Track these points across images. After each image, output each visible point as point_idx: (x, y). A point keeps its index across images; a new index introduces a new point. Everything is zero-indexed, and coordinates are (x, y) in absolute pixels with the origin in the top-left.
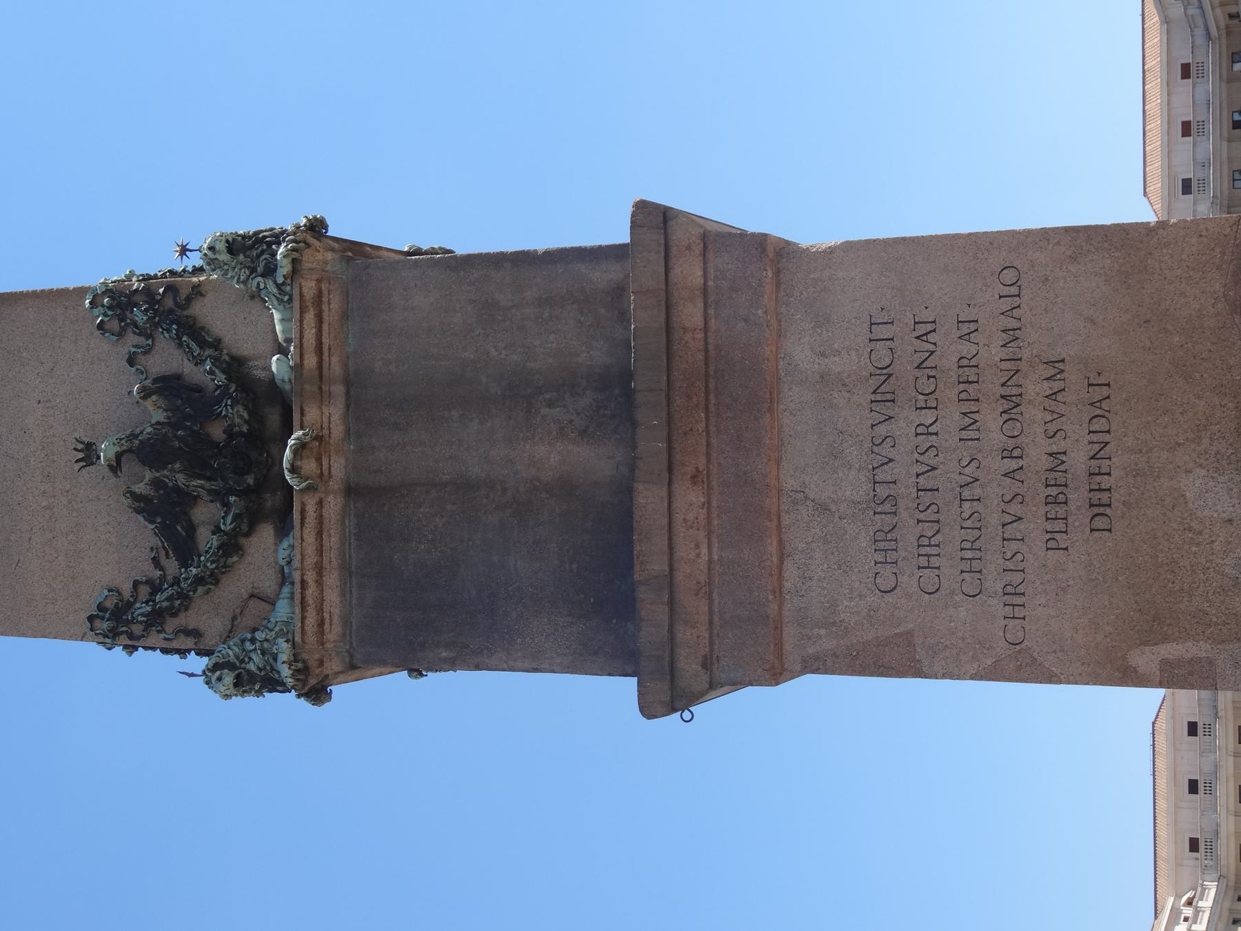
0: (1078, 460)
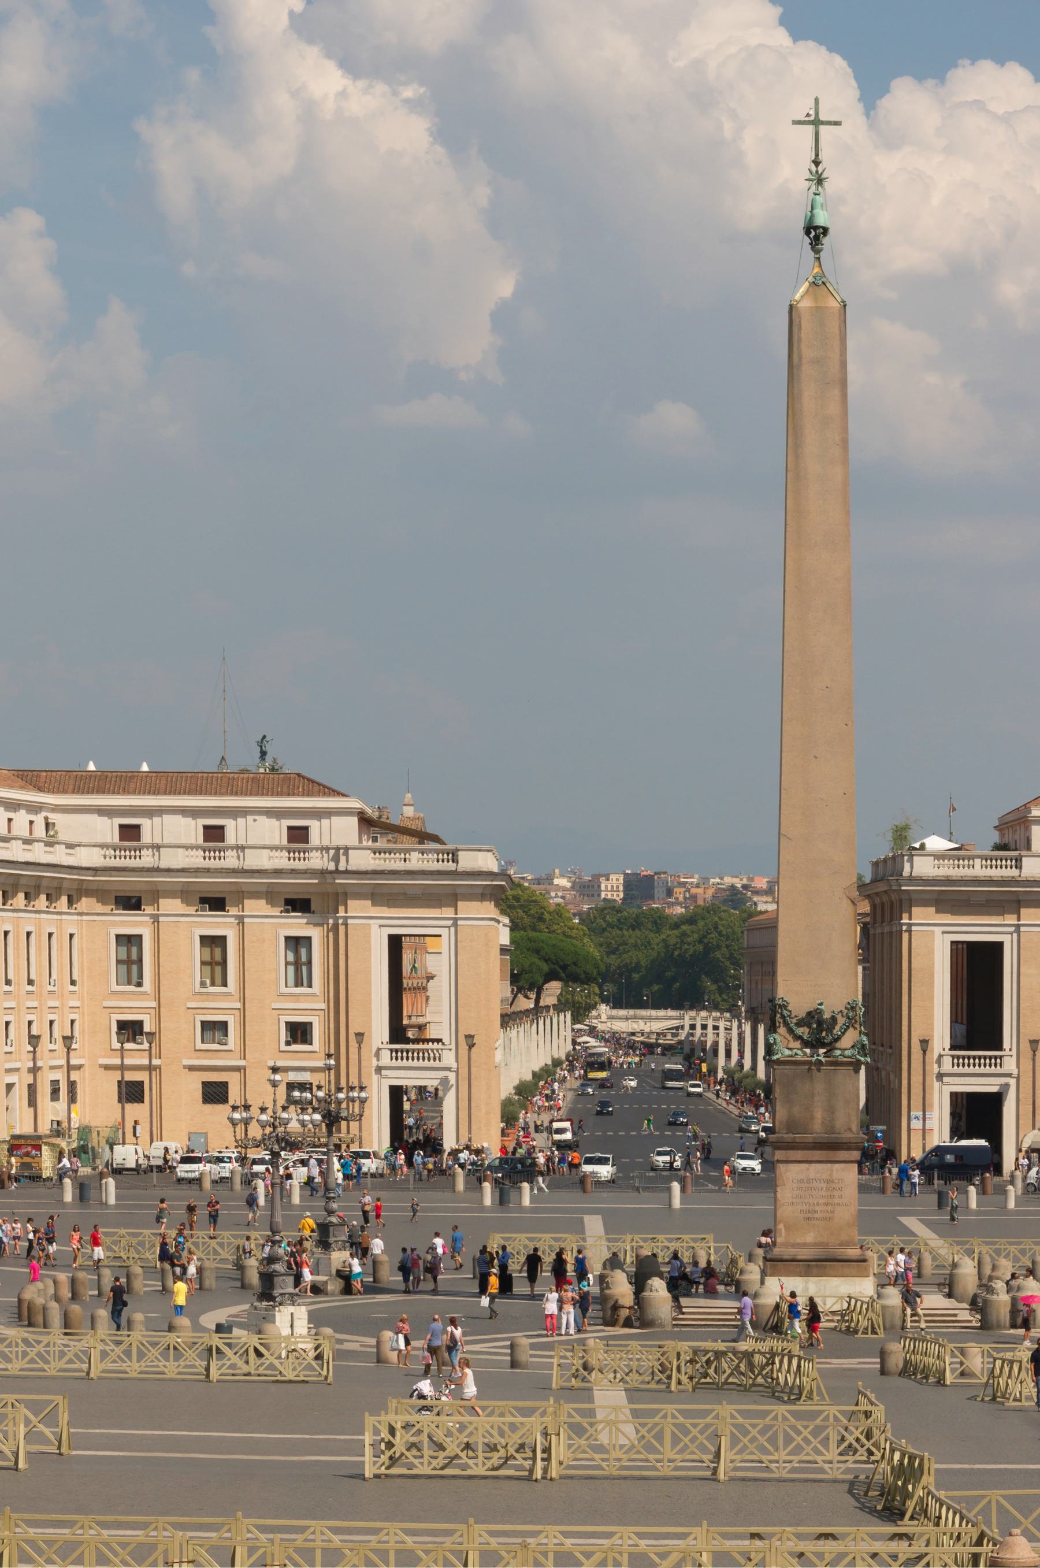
0: (816, 1216)
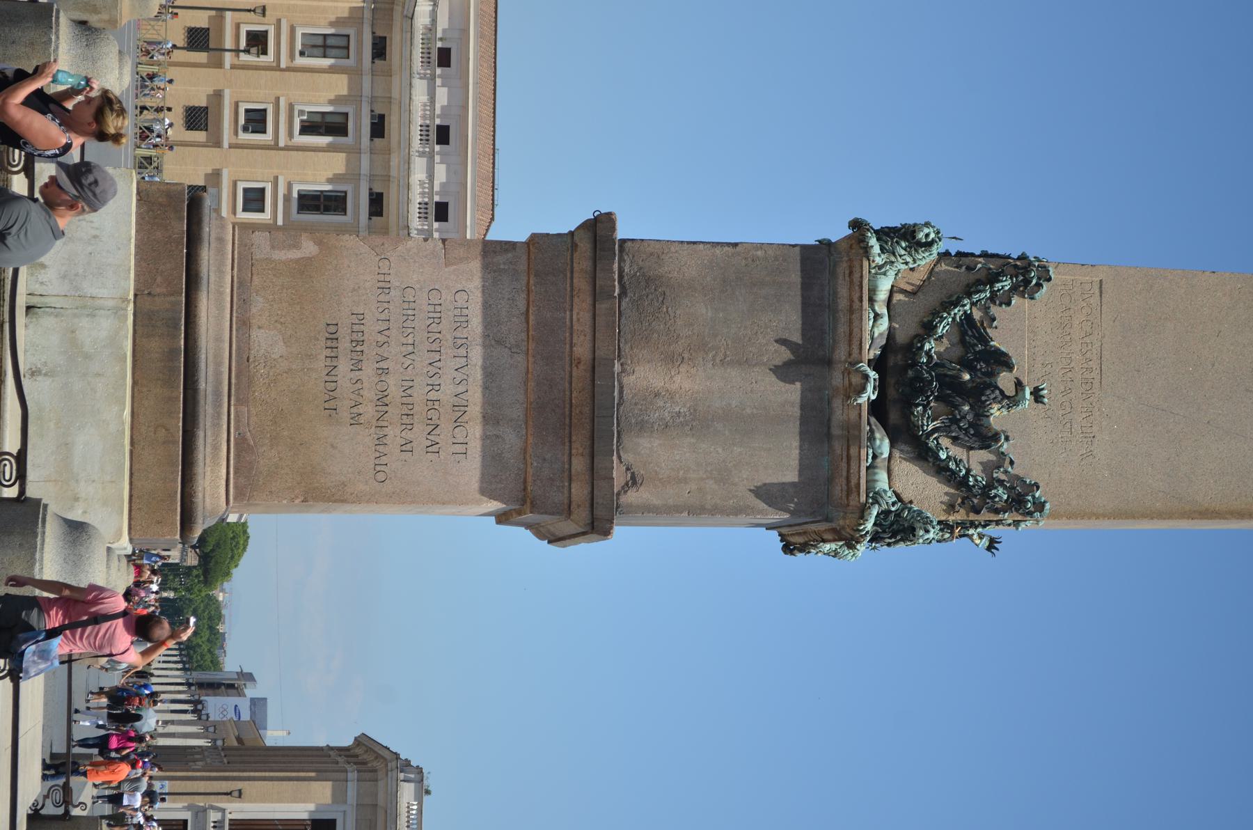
0: (344, 366)
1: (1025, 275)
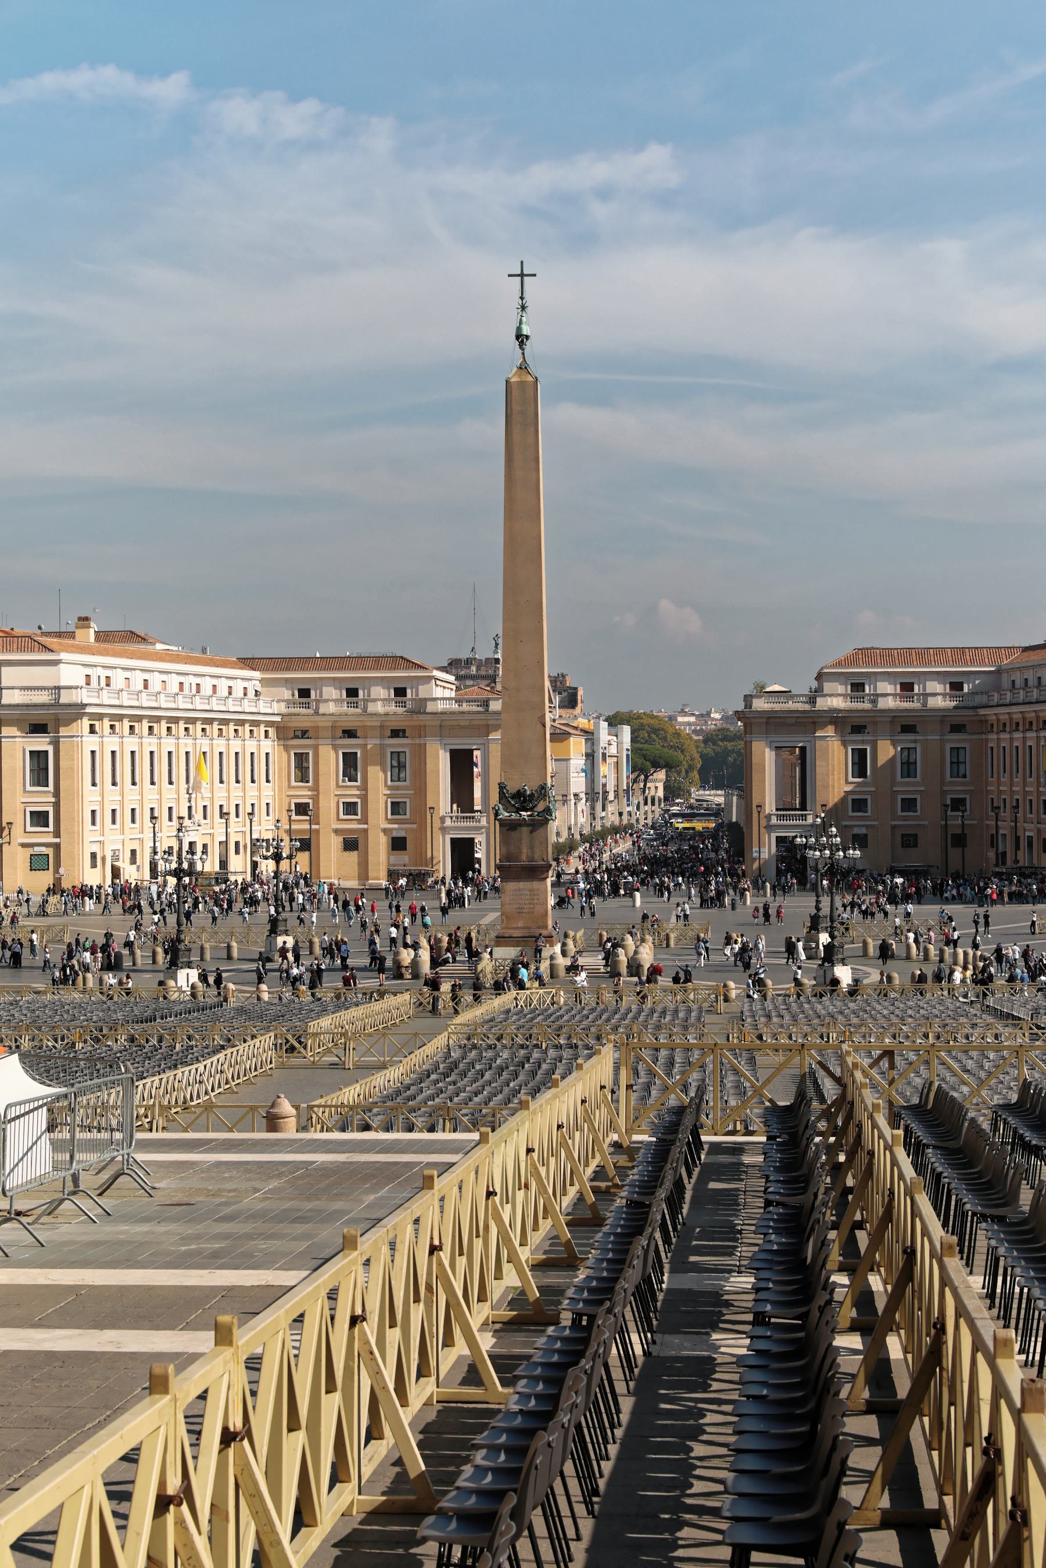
1: (502, 787)
